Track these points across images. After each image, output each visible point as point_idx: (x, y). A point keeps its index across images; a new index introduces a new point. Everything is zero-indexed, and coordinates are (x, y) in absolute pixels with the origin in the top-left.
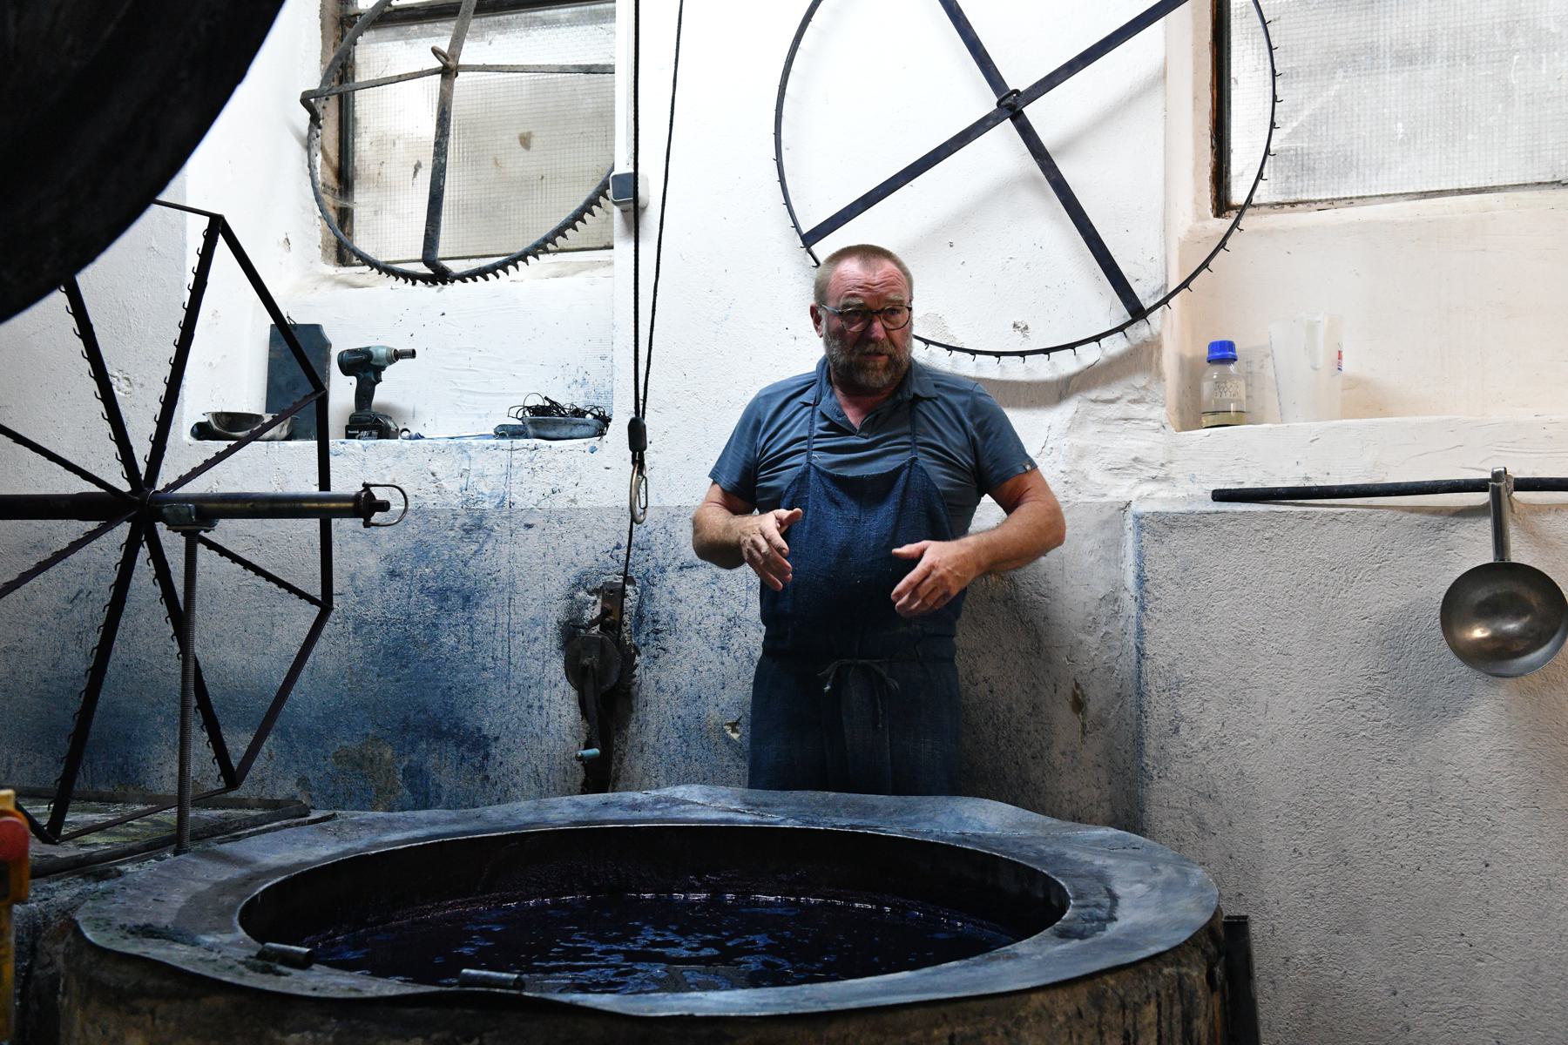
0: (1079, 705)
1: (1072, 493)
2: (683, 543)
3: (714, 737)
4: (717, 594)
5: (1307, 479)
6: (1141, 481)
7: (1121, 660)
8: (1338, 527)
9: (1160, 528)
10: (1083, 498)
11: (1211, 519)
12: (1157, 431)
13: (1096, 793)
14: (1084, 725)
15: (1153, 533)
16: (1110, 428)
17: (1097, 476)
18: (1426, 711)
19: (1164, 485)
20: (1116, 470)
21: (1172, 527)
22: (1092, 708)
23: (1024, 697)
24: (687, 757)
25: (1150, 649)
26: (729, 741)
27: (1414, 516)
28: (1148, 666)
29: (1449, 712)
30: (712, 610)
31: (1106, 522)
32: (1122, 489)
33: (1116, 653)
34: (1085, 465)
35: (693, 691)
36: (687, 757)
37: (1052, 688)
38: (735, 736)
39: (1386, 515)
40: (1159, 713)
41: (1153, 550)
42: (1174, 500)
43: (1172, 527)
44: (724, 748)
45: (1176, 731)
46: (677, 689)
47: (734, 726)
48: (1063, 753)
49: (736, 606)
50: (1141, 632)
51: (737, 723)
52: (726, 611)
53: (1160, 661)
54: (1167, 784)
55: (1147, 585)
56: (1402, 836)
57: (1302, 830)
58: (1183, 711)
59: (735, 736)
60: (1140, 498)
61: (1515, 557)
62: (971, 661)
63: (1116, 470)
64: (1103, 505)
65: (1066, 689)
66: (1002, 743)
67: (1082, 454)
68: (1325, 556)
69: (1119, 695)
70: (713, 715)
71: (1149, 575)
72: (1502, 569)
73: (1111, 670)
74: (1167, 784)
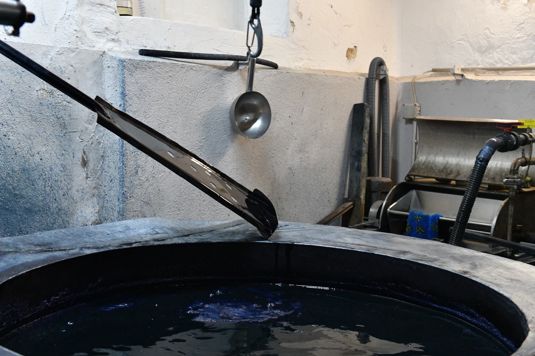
0: (85, 163)
1: (79, 43)
5: (169, 48)
6: (108, 41)
7: (103, 137)
8: (192, 72)
9: (132, 67)
10: (84, 47)
11: (151, 65)
12: (113, 13)
13: (92, 210)
14: (87, 174)
15: (129, 70)
16: (94, 8)
17: (91, 36)
19: (117, 44)
20: (98, 33)
21: (137, 68)
22: (91, 165)
23: (57, 161)
27: (215, 69)
31: (95, 62)
32: (102, 44)
33: (101, 134)
34: (85, 28)
37: (71, 155)
39: (207, 68)
41: (128, 80)
42: (122, 52)
43: (137, 68)
48: (77, 191)
54: (133, 200)
55: (127, 98)
56: (207, 208)
57: (178, 213)
58: (139, 162)
60: (109, 50)
61: (254, 90)
62: (30, 141)
63: (98, 33)
64: (94, 52)
65: (79, 155)
66: (48, 189)
67: (83, 21)
68: (188, 86)
69: (102, 156)
71: (127, 92)
72: (250, 94)
73: (99, 143)
74: (133, 200)
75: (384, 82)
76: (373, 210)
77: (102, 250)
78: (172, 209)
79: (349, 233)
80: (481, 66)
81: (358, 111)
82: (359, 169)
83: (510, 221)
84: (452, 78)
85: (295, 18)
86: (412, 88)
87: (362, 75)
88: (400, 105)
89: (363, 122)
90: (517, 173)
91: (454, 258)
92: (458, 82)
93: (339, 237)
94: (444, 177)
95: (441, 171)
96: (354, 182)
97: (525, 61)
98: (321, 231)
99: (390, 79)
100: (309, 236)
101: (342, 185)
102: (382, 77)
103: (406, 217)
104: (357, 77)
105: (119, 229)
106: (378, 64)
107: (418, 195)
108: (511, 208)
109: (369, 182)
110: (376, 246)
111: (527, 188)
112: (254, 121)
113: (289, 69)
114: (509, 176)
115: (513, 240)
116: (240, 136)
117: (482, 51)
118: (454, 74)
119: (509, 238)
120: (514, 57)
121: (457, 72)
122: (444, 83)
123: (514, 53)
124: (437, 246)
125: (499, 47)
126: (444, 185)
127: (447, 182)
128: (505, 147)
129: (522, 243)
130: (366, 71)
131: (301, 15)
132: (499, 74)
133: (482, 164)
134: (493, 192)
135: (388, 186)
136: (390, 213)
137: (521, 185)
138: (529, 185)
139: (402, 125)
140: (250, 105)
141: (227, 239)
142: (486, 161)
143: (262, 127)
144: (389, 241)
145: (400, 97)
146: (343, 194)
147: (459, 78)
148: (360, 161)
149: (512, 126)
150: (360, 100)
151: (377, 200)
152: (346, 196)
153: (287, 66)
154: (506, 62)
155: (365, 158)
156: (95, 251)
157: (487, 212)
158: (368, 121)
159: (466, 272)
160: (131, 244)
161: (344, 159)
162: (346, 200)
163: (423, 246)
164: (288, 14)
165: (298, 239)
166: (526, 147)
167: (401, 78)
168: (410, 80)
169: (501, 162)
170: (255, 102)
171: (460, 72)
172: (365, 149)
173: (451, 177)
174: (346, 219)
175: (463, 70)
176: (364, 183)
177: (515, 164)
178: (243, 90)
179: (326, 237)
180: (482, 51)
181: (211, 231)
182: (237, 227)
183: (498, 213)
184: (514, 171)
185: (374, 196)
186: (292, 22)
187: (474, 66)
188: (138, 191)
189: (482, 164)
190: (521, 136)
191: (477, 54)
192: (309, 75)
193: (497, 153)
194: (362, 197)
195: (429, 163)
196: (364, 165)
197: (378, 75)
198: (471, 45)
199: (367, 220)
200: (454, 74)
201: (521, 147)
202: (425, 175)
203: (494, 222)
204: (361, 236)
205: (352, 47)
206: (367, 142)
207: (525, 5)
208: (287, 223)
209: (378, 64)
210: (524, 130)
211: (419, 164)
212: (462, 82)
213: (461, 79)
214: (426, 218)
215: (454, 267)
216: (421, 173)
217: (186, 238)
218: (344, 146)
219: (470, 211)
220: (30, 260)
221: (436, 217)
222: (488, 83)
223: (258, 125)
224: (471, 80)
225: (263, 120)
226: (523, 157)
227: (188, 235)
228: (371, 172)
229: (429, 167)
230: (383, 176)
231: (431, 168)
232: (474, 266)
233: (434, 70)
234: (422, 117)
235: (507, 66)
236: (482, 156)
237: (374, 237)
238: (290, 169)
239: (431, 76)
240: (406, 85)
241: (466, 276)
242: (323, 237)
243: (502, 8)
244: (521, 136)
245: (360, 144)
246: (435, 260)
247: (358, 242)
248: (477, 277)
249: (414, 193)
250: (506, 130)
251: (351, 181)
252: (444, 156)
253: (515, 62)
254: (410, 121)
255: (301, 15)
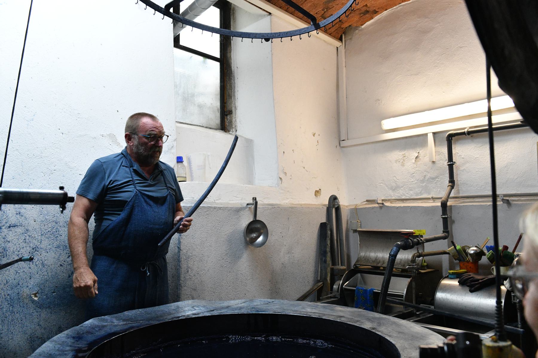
2: (10, 215)
3: (26, 301)
4: (28, 238)
8: (221, 211)
18: (235, 257)
24: (12, 312)
25: (182, 247)
26: (33, 301)
28: (181, 252)
29: (239, 257)
30: (25, 245)
35: (16, 281)
36: (12, 312)
38: (36, 299)
40: (184, 266)
44: (31, 305)
45: (188, 271)
46: (7, 282)
47: (35, 295)
49: (36, 242)
50: (180, 243)
51: (36, 294)
52: (32, 245)
53: (184, 251)
58: (189, 265)
59: (36, 299)
70: (26, 291)
75: (338, 209)
76: (335, 287)
77: (162, 322)
78: (210, 292)
79: (309, 305)
80: (393, 198)
81: (323, 226)
82: (325, 262)
83: (414, 291)
84: (377, 205)
85: (282, 176)
86: (355, 211)
87: (325, 205)
88: (349, 222)
89: (326, 233)
90: (415, 262)
91: (369, 319)
92: (381, 207)
93: (303, 308)
94: (375, 265)
95: (374, 262)
96: (323, 270)
97: (417, 194)
98: (293, 305)
99: (341, 207)
100: (285, 308)
101: (316, 272)
102: (336, 206)
103: (354, 290)
104: (321, 207)
105: (173, 308)
106: (334, 199)
107: (362, 276)
108: (414, 283)
109: (332, 269)
110: (325, 313)
111: (425, 270)
112: (258, 237)
113: (280, 205)
114: (410, 264)
115: (416, 303)
116: (250, 246)
117: (394, 189)
118: (378, 203)
119: (414, 302)
120: (411, 192)
121: (379, 202)
122: (373, 208)
123: (411, 190)
124: (360, 312)
125: (402, 187)
126: (375, 270)
127: (378, 268)
128: (406, 247)
129: (421, 305)
130: (327, 203)
131: (285, 173)
132: (403, 202)
133: (393, 257)
134: (403, 273)
135: (344, 271)
136: (345, 289)
137: (417, 269)
138: (426, 268)
139: (351, 234)
140: (256, 228)
141: (236, 312)
142: (395, 256)
143: (263, 240)
144: (332, 310)
145: (349, 217)
146: (317, 278)
147: (381, 205)
148: (325, 256)
149: (410, 234)
150: (324, 220)
151: (338, 280)
152: (319, 279)
153: (278, 203)
154: (407, 195)
155: (329, 254)
156: (157, 323)
157: (400, 286)
158: (329, 232)
159: (374, 329)
160: (179, 317)
161: (316, 256)
162: (318, 281)
163: (352, 312)
164: (278, 173)
165: (279, 311)
166: (419, 246)
167: (349, 205)
168: (353, 207)
169: (404, 256)
170: (259, 226)
171: (381, 202)
172: (328, 249)
173: (379, 265)
174: (318, 294)
175: (383, 200)
176: (329, 270)
177: (413, 257)
178: (252, 220)
179: (296, 309)
180: (394, 189)
181: (228, 307)
182: (243, 304)
183: (406, 287)
184: (413, 261)
185: (336, 278)
186: (280, 178)
187: (389, 198)
188: (189, 283)
189: (393, 257)
190: (415, 240)
191: (391, 191)
192: (292, 208)
193: (401, 251)
194: (328, 279)
195: (367, 257)
196: (329, 258)
197: (334, 205)
198: (387, 186)
199: (331, 293)
200: (378, 203)
201: (416, 247)
202: (365, 264)
203: (405, 292)
204: (317, 307)
205: (318, 189)
206: (329, 245)
207: (414, 163)
208: (273, 300)
209: (334, 199)
210: (417, 236)
211: (360, 257)
212: (383, 208)
213: (382, 206)
214: (366, 291)
215: (367, 326)
216: (362, 263)
217: (211, 312)
218: (316, 248)
219: (388, 287)
220: (119, 330)
221: (372, 290)
222: (397, 208)
223: (261, 239)
224: (388, 206)
225: (264, 237)
226: (418, 252)
227: (213, 310)
228: (334, 263)
229: (367, 259)
230: (341, 265)
231: (368, 260)
232: (380, 324)
233: (367, 201)
234: (360, 229)
235: (408, 198)
236: (392, 253)
237: (324, 307)
238: (283, 264)
239: (366, 204)
240: (352, 210)
241: (373, 331)
242: (294, 309)
243: (402, 165)
244: (415, 240)
245: (325, 247)
246: (358, 321)
247: (314, 311)
248: (379, 331)
249: (359, 275)
250: (406, 237)
251: (321, 269)
252: (375, 253)
253: (412, 195)
254: (355, 231)
255: (285, 173)
